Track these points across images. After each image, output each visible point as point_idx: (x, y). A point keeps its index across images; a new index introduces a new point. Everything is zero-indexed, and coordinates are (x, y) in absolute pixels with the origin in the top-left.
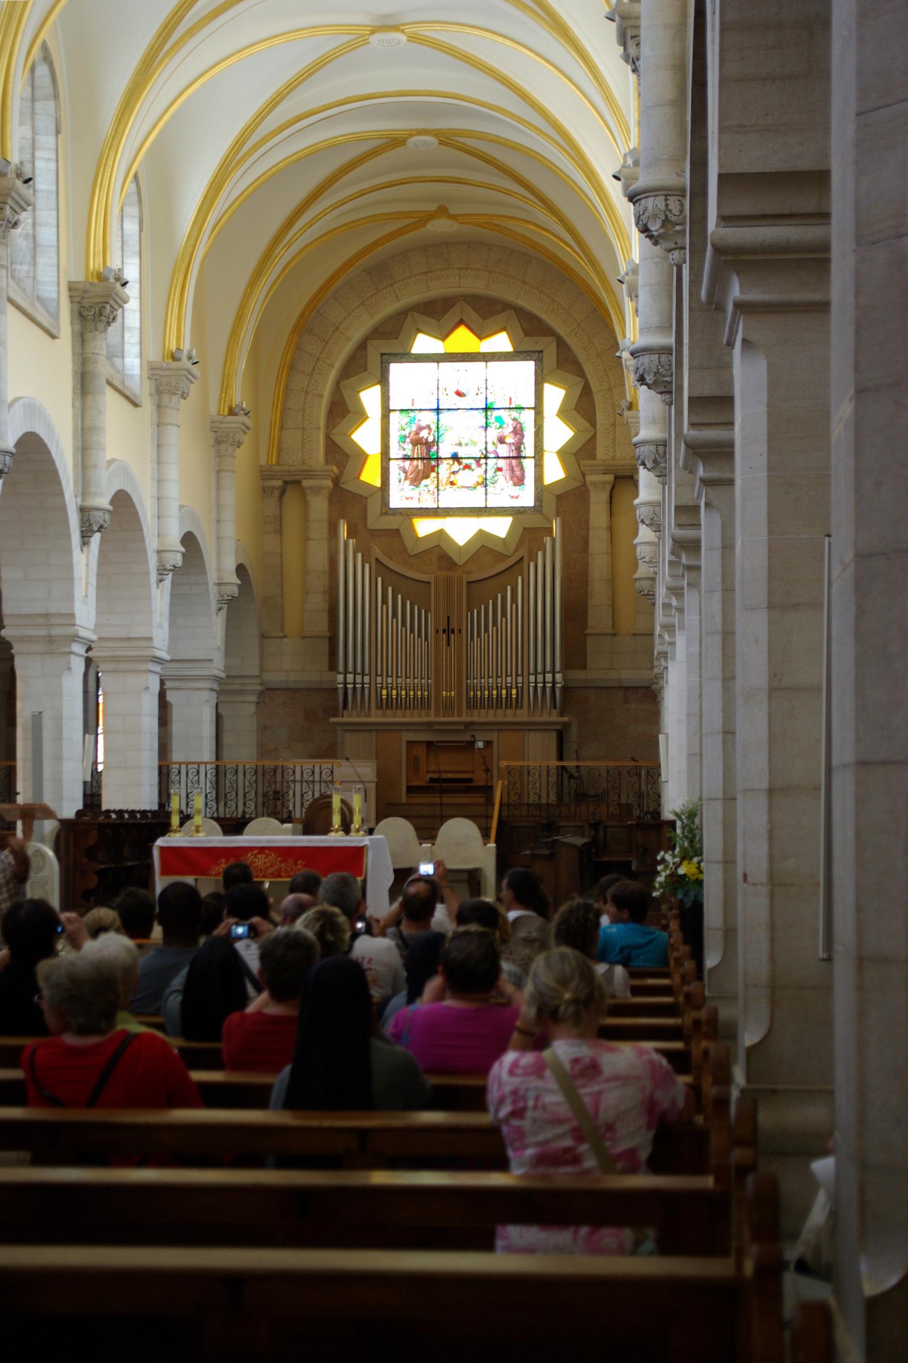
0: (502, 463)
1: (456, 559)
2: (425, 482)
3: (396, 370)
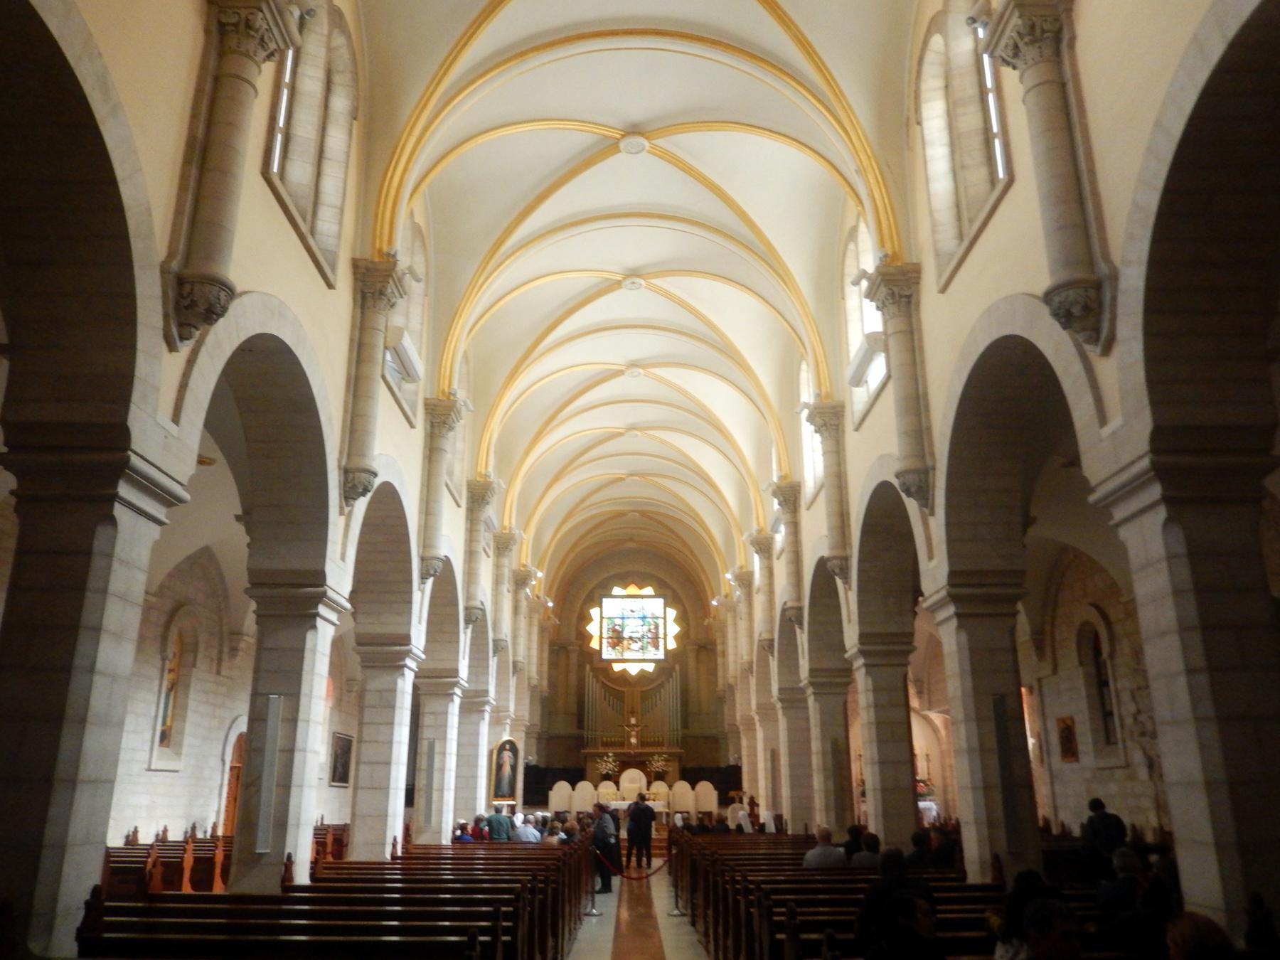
0: (649, 640)
1: (631, 680)
2: (617, 648)
3: (605, 601)
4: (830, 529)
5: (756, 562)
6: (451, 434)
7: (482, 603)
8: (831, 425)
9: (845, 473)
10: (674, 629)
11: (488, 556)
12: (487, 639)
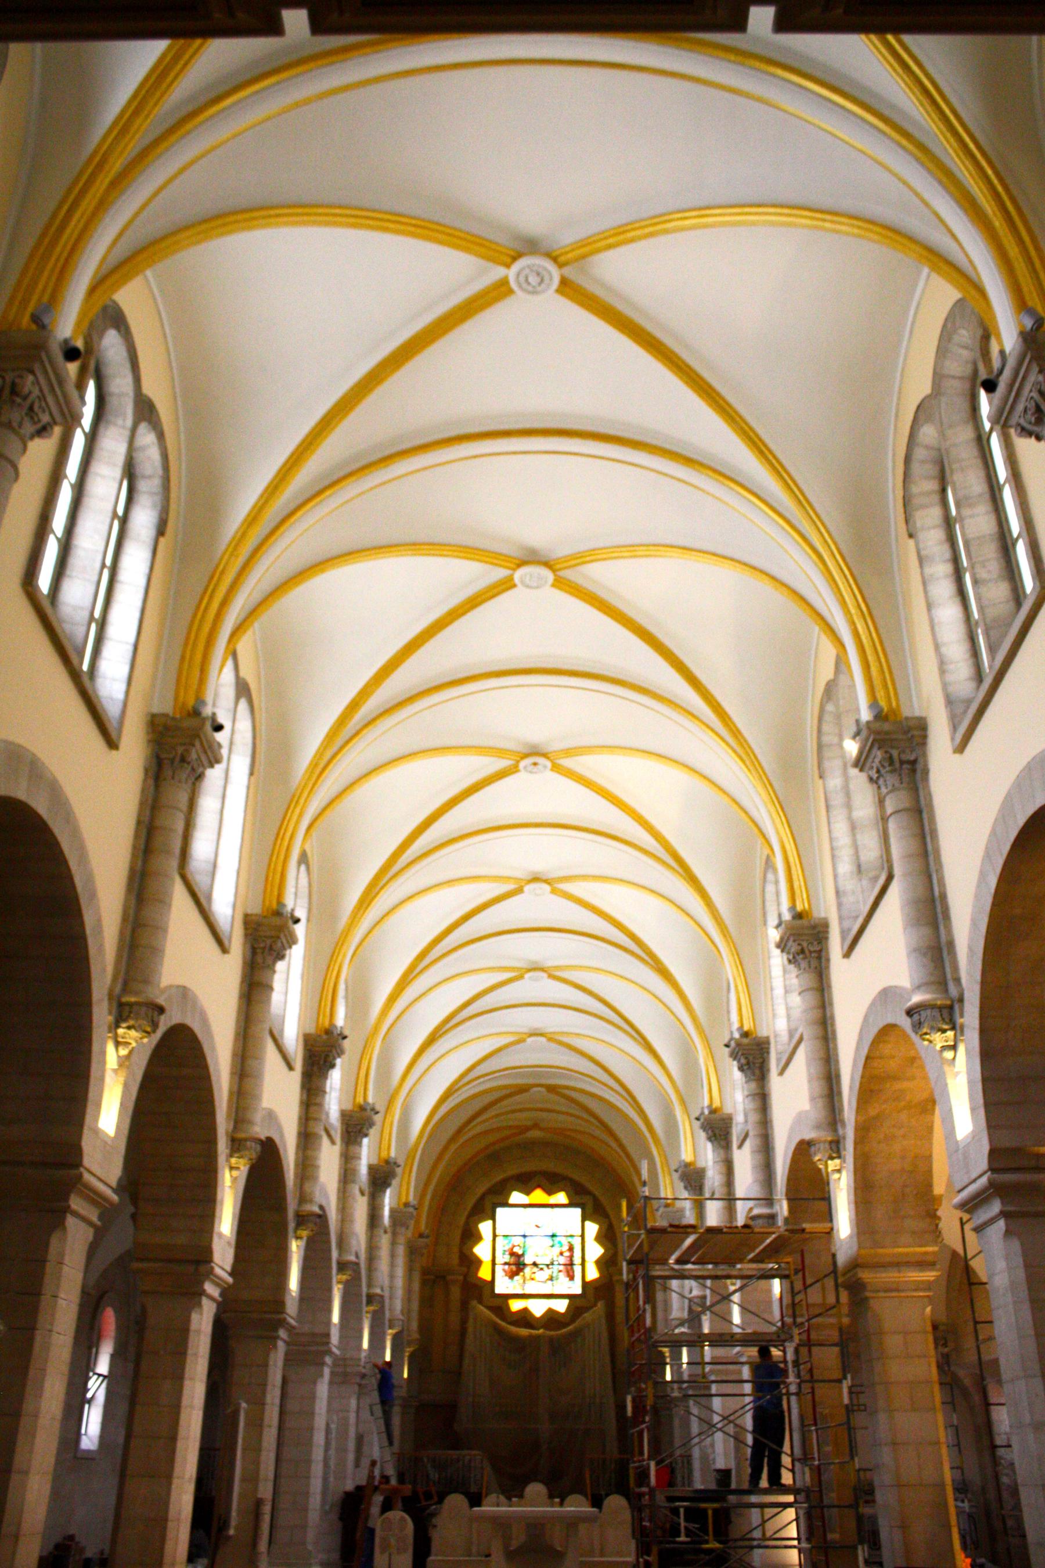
0: (562, 1268)
2: (516, 1278)
3: (500, 1212)
4: (812, 1099)
5: (708, 1157)
6: (280, 966)
7: (321, 1207)
8: (811, 952)
9: (832, 1018)
10: (595, 1251)
11: (333, 1142)
12: (330, 1259)
